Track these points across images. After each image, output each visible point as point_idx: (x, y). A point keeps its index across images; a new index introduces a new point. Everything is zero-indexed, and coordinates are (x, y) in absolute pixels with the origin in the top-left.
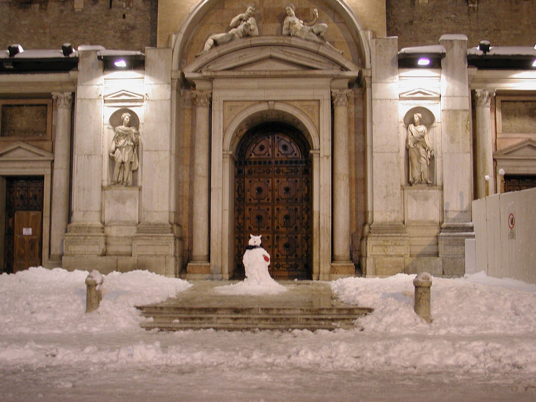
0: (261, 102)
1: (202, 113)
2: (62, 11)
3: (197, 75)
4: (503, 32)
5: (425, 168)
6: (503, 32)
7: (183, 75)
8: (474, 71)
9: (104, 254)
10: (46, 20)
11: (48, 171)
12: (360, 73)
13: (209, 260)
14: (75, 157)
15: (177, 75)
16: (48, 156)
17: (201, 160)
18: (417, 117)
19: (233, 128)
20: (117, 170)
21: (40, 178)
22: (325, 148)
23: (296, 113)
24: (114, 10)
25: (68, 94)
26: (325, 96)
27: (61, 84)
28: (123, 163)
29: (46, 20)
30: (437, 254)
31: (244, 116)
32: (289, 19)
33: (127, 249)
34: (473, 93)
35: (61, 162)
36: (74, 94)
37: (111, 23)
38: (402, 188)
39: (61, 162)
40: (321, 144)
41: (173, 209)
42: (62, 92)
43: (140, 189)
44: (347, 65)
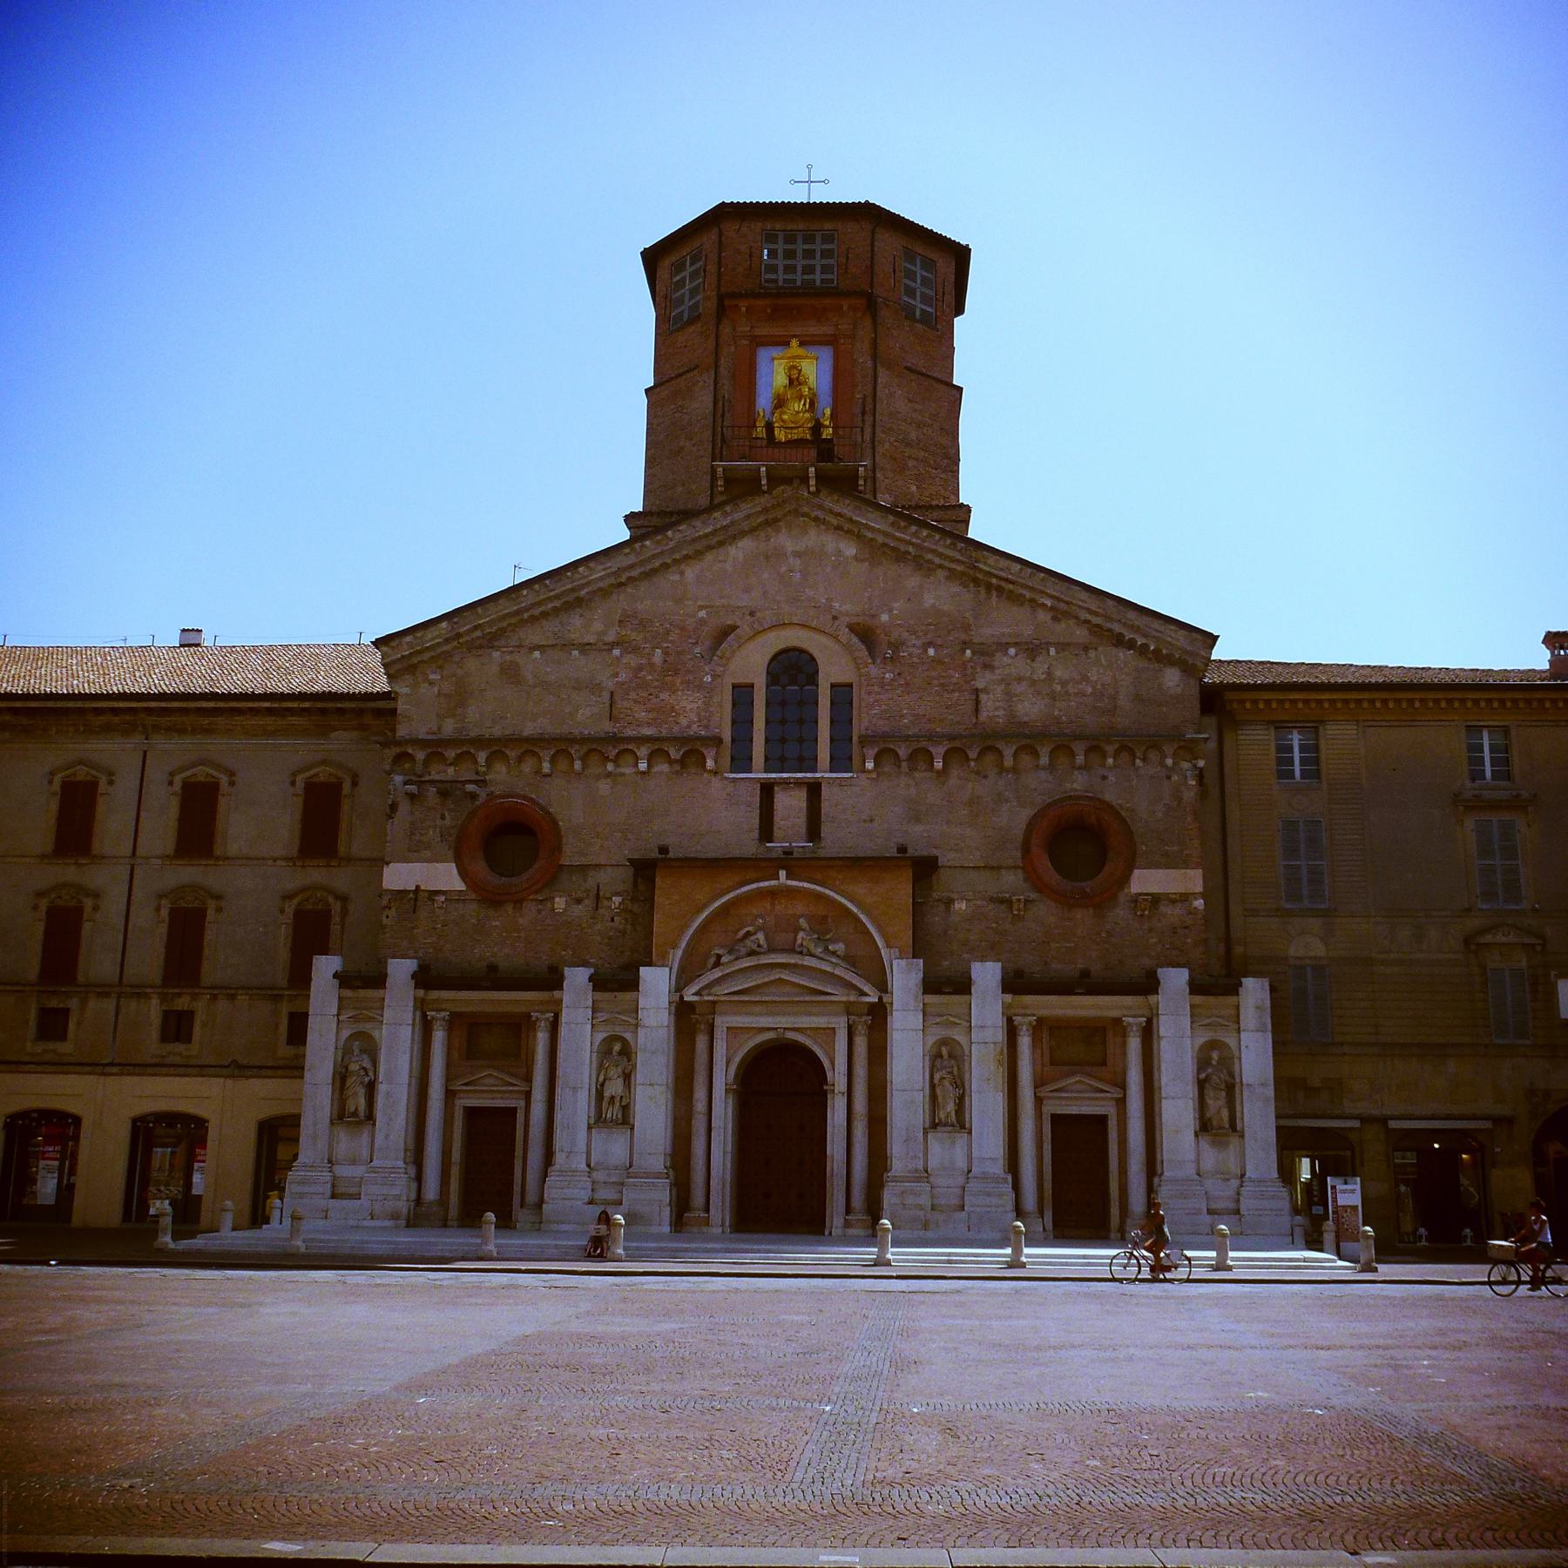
0: (769, 1029)
1: (701, 1042)
2: (539, 911)
3: (696, 998)
4: (1053, 945)
5: (951, 1107)
6: (1053, 945)
7: (682, 997)
8: (1009, 998)
9: (591, 1202)
10: (521, 921)
11: (522, 1103)
12: (880, 998)
13: (708, 1211)
14: (558, 1091)
15: (676, 997)
17: (700, 1094)
18: (944, 1051)
19: (737, 1059)
21: (512, 1112)
22: (840, 1083)
23: (808, 1042)
24: (601, 911)
26: (840, 1024)
27: (542, 1003)
28: (613, 1098)
29: (521, 921)
30: (962, 1208)
31: (751, 1044)
32: (801, 935)
33: (615, 1196)
34: (1010, 1020)
35: (539, 1094)
36: (557, 1017)
37: (599, 927)
38: (925, 1133)
39: (539, 1094)
40: (837, 1078)
41: (669, 1150)
42: (543, 1013)
43: (632, 1129)
44: (867, 988)
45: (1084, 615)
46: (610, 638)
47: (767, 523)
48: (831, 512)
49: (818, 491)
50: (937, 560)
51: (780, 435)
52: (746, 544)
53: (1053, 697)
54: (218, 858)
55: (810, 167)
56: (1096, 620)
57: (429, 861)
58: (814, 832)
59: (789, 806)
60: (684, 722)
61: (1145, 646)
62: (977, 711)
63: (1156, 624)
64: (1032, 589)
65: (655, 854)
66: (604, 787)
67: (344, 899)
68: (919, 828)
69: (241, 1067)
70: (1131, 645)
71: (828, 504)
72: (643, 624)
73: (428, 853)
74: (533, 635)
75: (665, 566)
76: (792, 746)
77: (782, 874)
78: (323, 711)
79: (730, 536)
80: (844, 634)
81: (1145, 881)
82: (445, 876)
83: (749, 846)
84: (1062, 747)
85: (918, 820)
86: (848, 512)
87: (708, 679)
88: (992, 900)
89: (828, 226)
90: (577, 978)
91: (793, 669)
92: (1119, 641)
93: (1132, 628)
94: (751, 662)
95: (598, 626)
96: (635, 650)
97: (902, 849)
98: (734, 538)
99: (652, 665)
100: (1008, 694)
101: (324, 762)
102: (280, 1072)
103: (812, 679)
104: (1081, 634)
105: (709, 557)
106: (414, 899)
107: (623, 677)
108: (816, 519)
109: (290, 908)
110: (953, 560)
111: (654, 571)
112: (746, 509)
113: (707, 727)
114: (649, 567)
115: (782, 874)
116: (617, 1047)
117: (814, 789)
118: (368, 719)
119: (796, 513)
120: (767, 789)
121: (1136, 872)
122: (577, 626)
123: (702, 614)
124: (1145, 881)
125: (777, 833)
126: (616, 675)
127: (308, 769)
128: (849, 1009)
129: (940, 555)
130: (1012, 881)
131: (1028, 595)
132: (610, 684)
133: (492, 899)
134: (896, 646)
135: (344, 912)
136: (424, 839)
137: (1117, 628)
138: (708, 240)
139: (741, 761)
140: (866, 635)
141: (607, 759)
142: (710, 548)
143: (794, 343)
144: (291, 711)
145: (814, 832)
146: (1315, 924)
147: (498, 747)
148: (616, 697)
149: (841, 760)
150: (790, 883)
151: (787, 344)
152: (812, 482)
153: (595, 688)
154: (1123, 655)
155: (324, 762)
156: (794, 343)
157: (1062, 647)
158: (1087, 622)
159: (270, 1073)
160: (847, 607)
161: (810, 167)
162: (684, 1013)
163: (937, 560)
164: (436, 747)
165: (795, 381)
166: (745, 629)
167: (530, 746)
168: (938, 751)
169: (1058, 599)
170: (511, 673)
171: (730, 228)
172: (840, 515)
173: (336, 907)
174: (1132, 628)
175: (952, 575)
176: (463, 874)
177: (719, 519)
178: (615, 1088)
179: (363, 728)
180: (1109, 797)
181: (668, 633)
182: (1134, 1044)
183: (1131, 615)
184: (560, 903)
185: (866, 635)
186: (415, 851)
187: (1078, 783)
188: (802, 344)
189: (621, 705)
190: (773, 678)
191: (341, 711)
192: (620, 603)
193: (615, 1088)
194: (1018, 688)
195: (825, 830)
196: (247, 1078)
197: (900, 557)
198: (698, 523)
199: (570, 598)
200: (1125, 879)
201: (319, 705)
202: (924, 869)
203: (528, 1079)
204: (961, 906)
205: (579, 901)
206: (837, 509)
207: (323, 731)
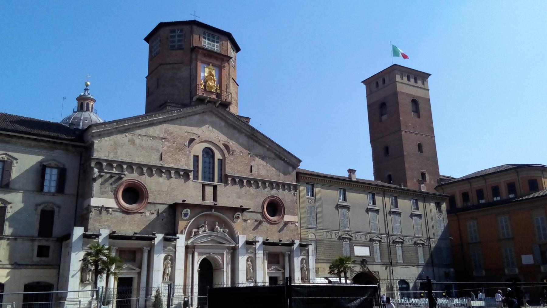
1: (190, 257)
8: (264, 246)
16: (138, 270)
20: (166, 276)
25: (149, 248)
45: (275, 151)
46: (161, 136)
47: (203, 112)
48: (220, 113)
49: (218, 107)
50: (244, 131)
51: (207, 89)
52: (197, 117)
53: (267, 170)
54: (11, 189)
55: (195, 12)
56: (277, 153)
57: (105, 198)
58: (215, 199)
59: (209, 190)
60: (182, 164)
61: (286, 161)
62: (251, 171)
63: (290, 156)
64: (265, 142)
65: (182, 202)
66: (161, 180)
67: (59, 207)
68: (240, 200)
69: (19, 265)
70: (283, 160)
71: (220, 111)
72: (171, 134)
73: (106, 195)
74: (139, 132)
75: (177, 119)
76: (209, 175)
77: (213, 210)
78: (55, 143)
79: (195, 114)
80: (222, 147)
81: (287, 218)
82: (111, 203)
83: (199, 201)
84: (271, 183)
85: (239, 198)
86: (225, 114)
87: (188, 152)
88: (256, 221)
89: (218, 35)
90: (159, 237)
91: (209, 153)
92: (281, 158)
93: (285, 156)
94: (198, 149)
95: (157, 132)
96: (168, 141)
97: (241, 206)
98: (195, 114)
99: (173, 146)
100: (258, 169)
101: (54, 160)
102: (34, 267)
103: (213, 156)
104: (273, 156)
105: (188, 118)
106: (101, 209)
107: (165, 148)
108: (216, 115)
109: (40, 209)
110: (247, 131)
111: (174, 119)
112: (200, 108)
113: (187, 166)
114: (173, 118)
115: (213, 210)
116: (170, 258)
117: (215, 187)
118: (70, 148)
119: (211, 111)
120: (204, 186)
121: (285, 216)
122: (151, 131)
123: (187, 134)
124: (287, 218)
125: (206, 198)
126: (163, 147)
127: (47, 161)
128: (228, 248)
129: (245, 130)
130: (259, 217)
131: (263, 144)
132: (161, 150)
133: (126, 212)
134: (234, 151)
135: (59, 212)
136: (105, 190)
137: (282, 156)
138: (186, 28)
139: (196, 177)
140: (226, 147)
141: (163, 172)
142: (189, 116)
143: (211, 65)
144: (43, 141)
145: (215, 199)
146: (313, 231)
147: (130, 166)
148: (163, 154)
149: (220, 180)
150: (215, 213)
151: (209, 65)
152: (218, 104)
153: (158, 150)
154: (282, 162)
155: (54, 160)
156: (211, 65)
157: (269, 158)
158: (275, 153)
159: (30, 267)
160: (222, 139)
161: (195, 12)
162: (187, 247)
163: (244, 131)
164: (110, 163)
165: (210, 74)
166: (197, 140)
167: (140, 167)
168: (245, 181)
169: (270, 146)
170: (132, 142)
171: (195, 28)
172: (223, 114)
173: (56, 209)
174: (285, 156)
175: (246, 135)
176: (118, 202)
177: (194, 109)
178: (169, 270)
179: (67, 150)
180: (279, 197)
181: (177, 138)
182: (287, 259)
183: (285, 153)
184: (148, 214)
185: (226, 147)
186: (102, 194)
187: (274, 192)
188: (212, 65)
189: (164, 157)
190: (203, 155)
191: (61, 143)
192: (164, 126)
193: (169, 270)
194: (261, 167)
195: (218, 198)
196: (21, 269)
197: (234, 128)
198: (188, 108)
199: (152, 122)
200: (283, 217)
201: (55, 140)
202: (242, 210)
203: (140, 267)
204: (249, 221)
205: (153, 214)
206: (222, 113)
207: (53, 149)
